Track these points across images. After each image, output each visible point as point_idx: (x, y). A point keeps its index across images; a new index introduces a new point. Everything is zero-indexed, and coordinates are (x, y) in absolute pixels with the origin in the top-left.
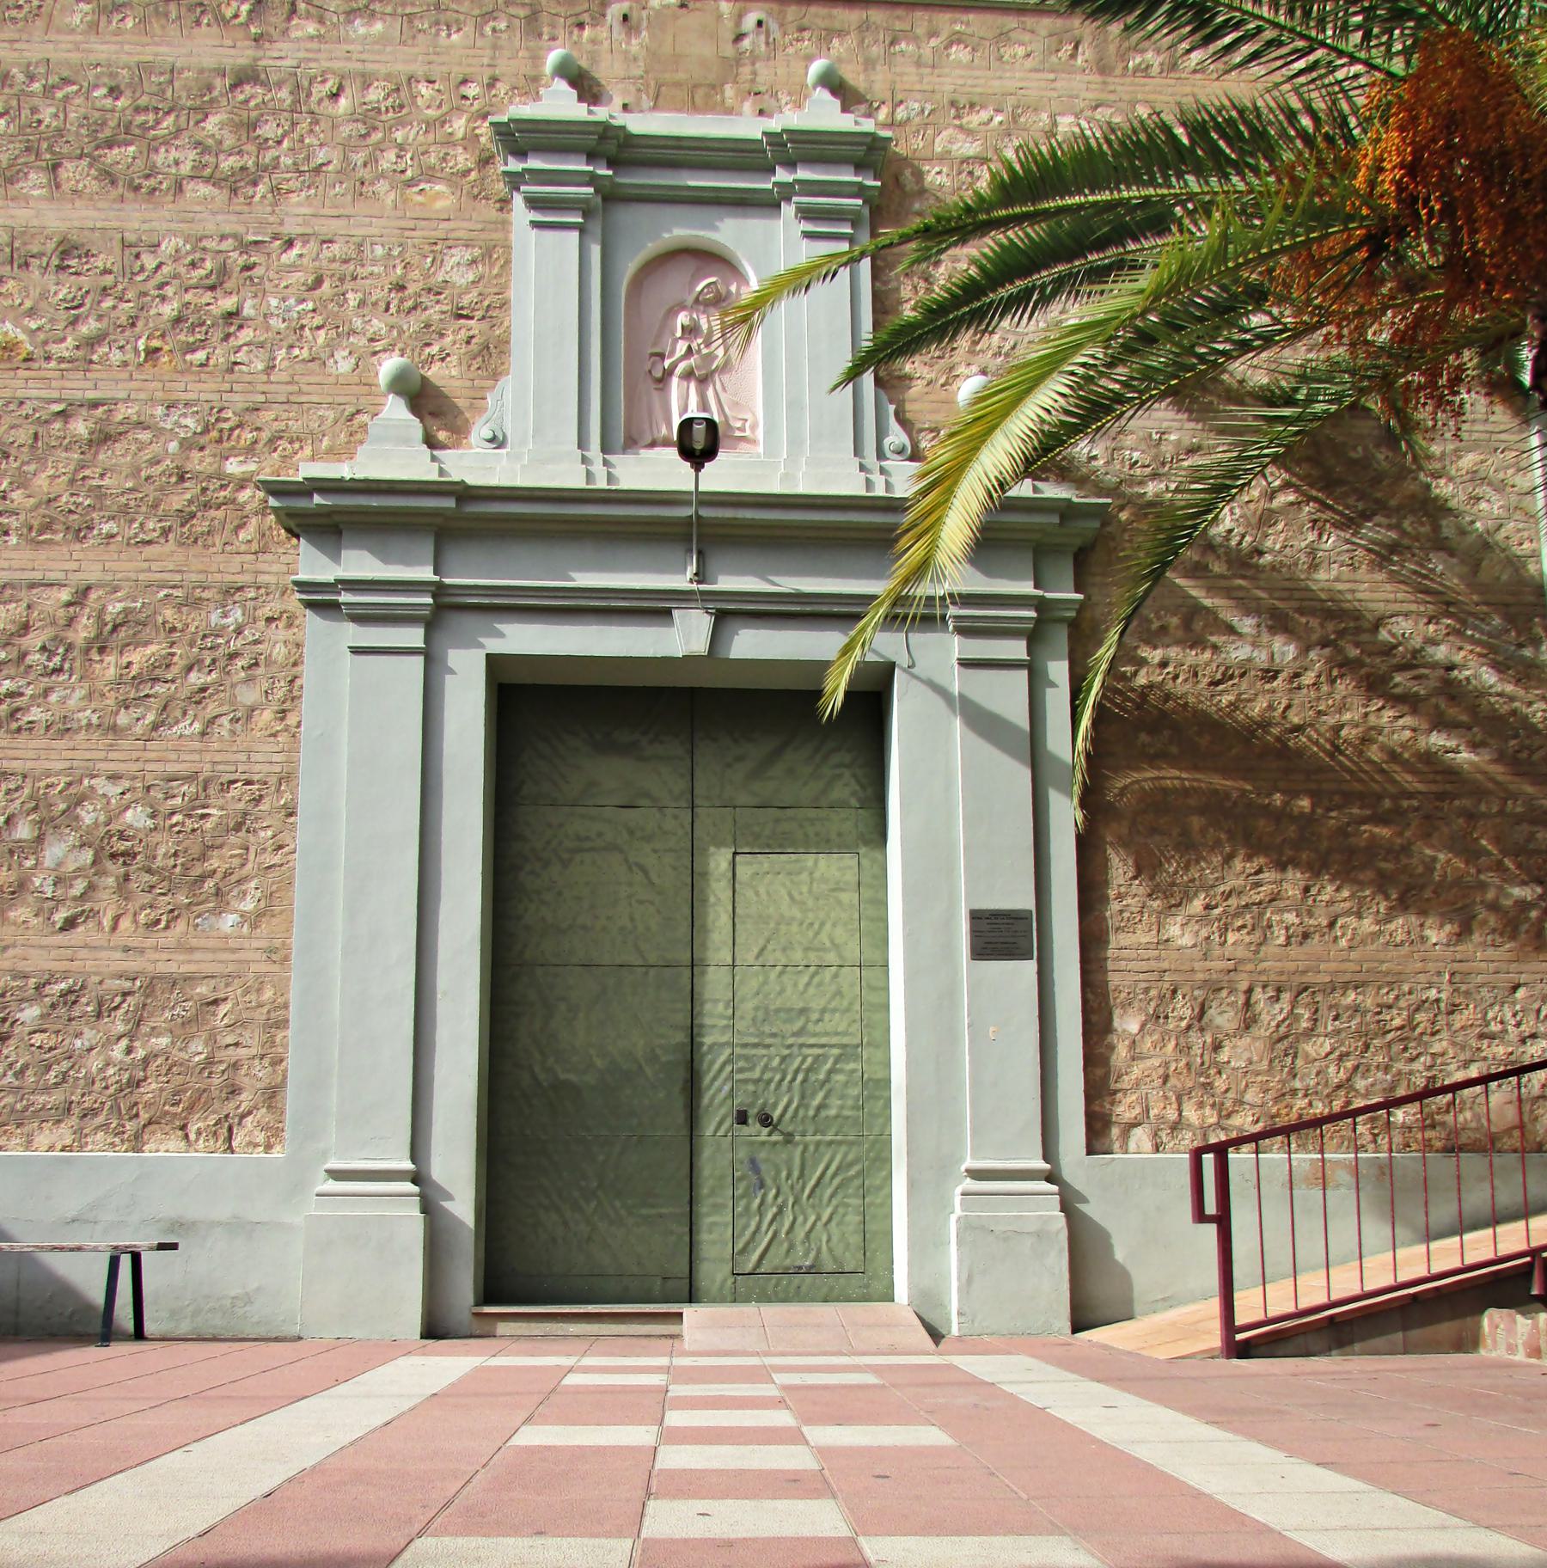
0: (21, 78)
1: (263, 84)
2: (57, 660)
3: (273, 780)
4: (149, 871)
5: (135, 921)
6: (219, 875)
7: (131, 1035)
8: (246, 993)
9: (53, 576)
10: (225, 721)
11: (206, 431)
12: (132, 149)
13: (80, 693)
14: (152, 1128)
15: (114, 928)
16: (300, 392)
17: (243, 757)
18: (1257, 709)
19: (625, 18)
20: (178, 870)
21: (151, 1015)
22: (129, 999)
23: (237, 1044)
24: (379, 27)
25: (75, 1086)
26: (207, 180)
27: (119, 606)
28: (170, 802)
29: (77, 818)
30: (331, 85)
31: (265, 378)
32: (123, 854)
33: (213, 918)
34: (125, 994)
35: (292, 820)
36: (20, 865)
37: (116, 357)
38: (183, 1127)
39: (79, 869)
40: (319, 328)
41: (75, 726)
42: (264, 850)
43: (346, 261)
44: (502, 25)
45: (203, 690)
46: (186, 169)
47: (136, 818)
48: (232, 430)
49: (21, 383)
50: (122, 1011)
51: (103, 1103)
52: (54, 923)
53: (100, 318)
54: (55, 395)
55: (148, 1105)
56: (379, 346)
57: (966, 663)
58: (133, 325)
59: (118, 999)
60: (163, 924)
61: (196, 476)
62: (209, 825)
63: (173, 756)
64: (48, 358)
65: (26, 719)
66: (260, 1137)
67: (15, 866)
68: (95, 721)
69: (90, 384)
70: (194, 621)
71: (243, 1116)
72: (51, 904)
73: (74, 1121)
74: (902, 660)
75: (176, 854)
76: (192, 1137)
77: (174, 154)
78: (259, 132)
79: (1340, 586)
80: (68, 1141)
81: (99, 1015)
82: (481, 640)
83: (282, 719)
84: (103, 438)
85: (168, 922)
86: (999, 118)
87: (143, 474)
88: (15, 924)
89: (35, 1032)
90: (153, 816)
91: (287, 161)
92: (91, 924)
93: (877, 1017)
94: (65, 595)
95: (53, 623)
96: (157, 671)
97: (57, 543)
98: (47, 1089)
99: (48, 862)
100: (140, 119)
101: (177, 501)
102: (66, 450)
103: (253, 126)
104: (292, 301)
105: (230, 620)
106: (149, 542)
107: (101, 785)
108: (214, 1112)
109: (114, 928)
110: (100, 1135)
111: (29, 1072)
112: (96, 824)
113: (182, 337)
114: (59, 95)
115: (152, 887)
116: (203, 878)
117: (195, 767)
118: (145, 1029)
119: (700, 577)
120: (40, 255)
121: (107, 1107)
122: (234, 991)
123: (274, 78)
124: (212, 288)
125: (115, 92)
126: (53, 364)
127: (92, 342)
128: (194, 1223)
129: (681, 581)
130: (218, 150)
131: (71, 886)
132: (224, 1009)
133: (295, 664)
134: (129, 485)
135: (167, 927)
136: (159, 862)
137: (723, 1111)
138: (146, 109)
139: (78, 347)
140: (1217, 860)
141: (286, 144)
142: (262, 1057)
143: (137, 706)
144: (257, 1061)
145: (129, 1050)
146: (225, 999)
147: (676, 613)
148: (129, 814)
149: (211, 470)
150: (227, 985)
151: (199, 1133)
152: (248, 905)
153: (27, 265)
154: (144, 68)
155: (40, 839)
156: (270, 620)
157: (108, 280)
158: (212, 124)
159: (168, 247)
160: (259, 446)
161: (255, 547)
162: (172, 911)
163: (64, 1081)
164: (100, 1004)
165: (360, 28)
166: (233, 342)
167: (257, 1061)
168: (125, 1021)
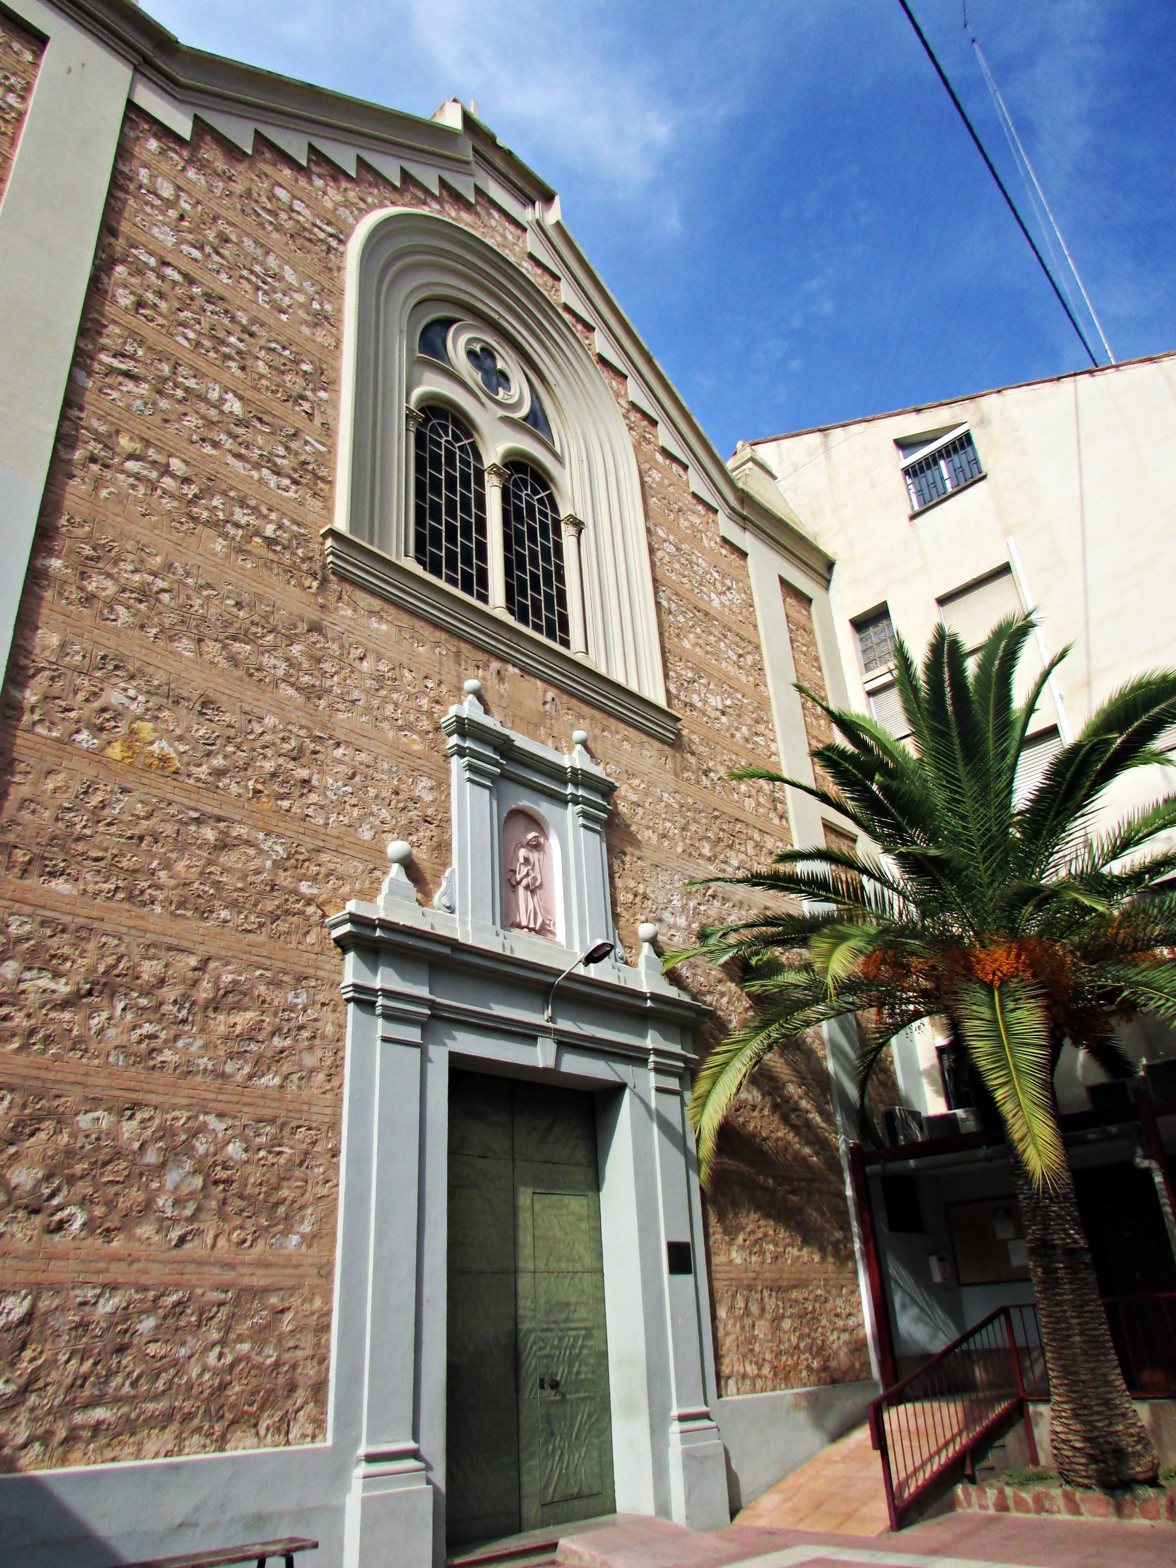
0: (181, 571)
1: (325, 636)
2: (185, 1012)
3: (324, 1128)
4: (241, 1196)
5: (229, 1240)
6: (287, 1203)
7: (222, 1342)
8: (304, 1301)
9: (185, 944)
10: (295, 1077)
11: (288, 858)
12: (248, 647)
13: (199, 1042)
14: (232, 1427)
15: (214, 1245)
16: (343, 846)
17: (305, 1107)
18: (751, 1126)
19: (499, 673)
20: (262, 1196)
21: (237, 1322)
22: (222, 1309)
23: (296, 1347)
24: (384, 627)
25: (177, 1393)
26: (292, 685)
27: (230, 977)
28: (258, 1140)
29: (193, 1147)
30: (359, 652)
31: (324, 830)
32: (224, 1182)
33: (283, 1239)
34: (221, 1304)
35: (334, 1160)
36: (147, 1186)
37: (235, 789)
38: (255, 1425)
39: (191, 1193)
40: (354, 806)
41: (195, 1069)
42: (317, 1183)
43: (368, 767)
44: (444, 652)
45: (282, 1052)
46: (280, 673)
47: (234, 1150)
48: (304, 861)
49: (170, 789)
50: (216, 1320)
51: (198, 1407)
52: (170, 1241)
53: (225, 757)
54: (192, 804)
55: (233, 1406)
56: (386, 827)
57: (659, 1090)
58: (246, 769)
59: (215, 1309)
60: (248, 1244)
61: (282, 888)
62: (282, 1160)
63: (261, 1102)
64: (189, 776)
65: (160, 1059)
66: (309, 1429)
67: (143, 1187)
68: (210, 1067)
69: (215, 803)
70: (278, 998)
71: (297, 1411)
72: (169, 1222)
73: (174, 1427)
74: (631, 1084)
75: (261, 1184)
76: (262, 1432)
77: (273, 661)
78: (322, 666)
79: (772, 1064)
80: (170, 1446)
81: (199, 1326)
82: (447, 1041)
83: (329, 1081)
84: (223, 845)
85: (253, 1241)
86: (643, 785)
87: (249, 879)
88: (139, 1239)
89: (149, 1342)
90: (246, 1150)
91: (337, 690)
92: (196, 1242)
93: (600, 1307)
94: (193, 961)
95: (183, 981)
96: (253, 1033)
97: (188, 918)
98: (156, 1398)
99: (169, 1185)
100: (254, 629)
101: (270, 905)
102: (199, 848)
103: (319, 661)
104: (340, 784)
105: (299, 1001)
106: (250, 931)
107: (212, 1121)
108: (279, 1409)
109: (214, 1245)
110: (196, 1437)
111: (142, 1381)
112: (207, 1154)
113: (276, 787)
114: (205, 593)
115: (242, 1210)
116: (277, 1204)
117: (276, 1112)
118: (232, 1336)
119: (551, 1019)
120: (189, 700)
121: (201, 1412)
122: (295, 1301)
123: (330, 635)
124: (294, 759)
125: (239, 605)
126: (192, 781)
127: (219, 773)
128: (270, 1515)
129: (540, 1019)
130: (297, 666)
131: (184, 1208)
132: (288, 1316)
133: (338, 1040)
134: (240, 885)
135: (251, 1246)
136: (249, 1190)
137: (532, 1380)
138: (257, 624)
139: (210, 774)
140: (745, 1212)
141: (336, 678)
142: (312, 1358)
143: (239, 1059)
144: (309, 1362)
145: (221, 1356)
146: (289, 1308)
147: (540, 1039)
148: (230, 1147)
149: (291, 886)
150: (291, 1296)
151: (268, 1429)
152: (306, 1228)
153: (178, 703)
154: (260, 598)
155: (163, 1165)
156: (323, 1004)
157: (232, 732)
158: (296, 649)
159: (270, 721)
160: (320, 877)
161: (317, 949)
162: (255, 1232)
163: (170, 1388)
164: (201, 1315)
165: (374, 623)
166: (304, 800)
167: (309, 1362)
168: (219, 1329)
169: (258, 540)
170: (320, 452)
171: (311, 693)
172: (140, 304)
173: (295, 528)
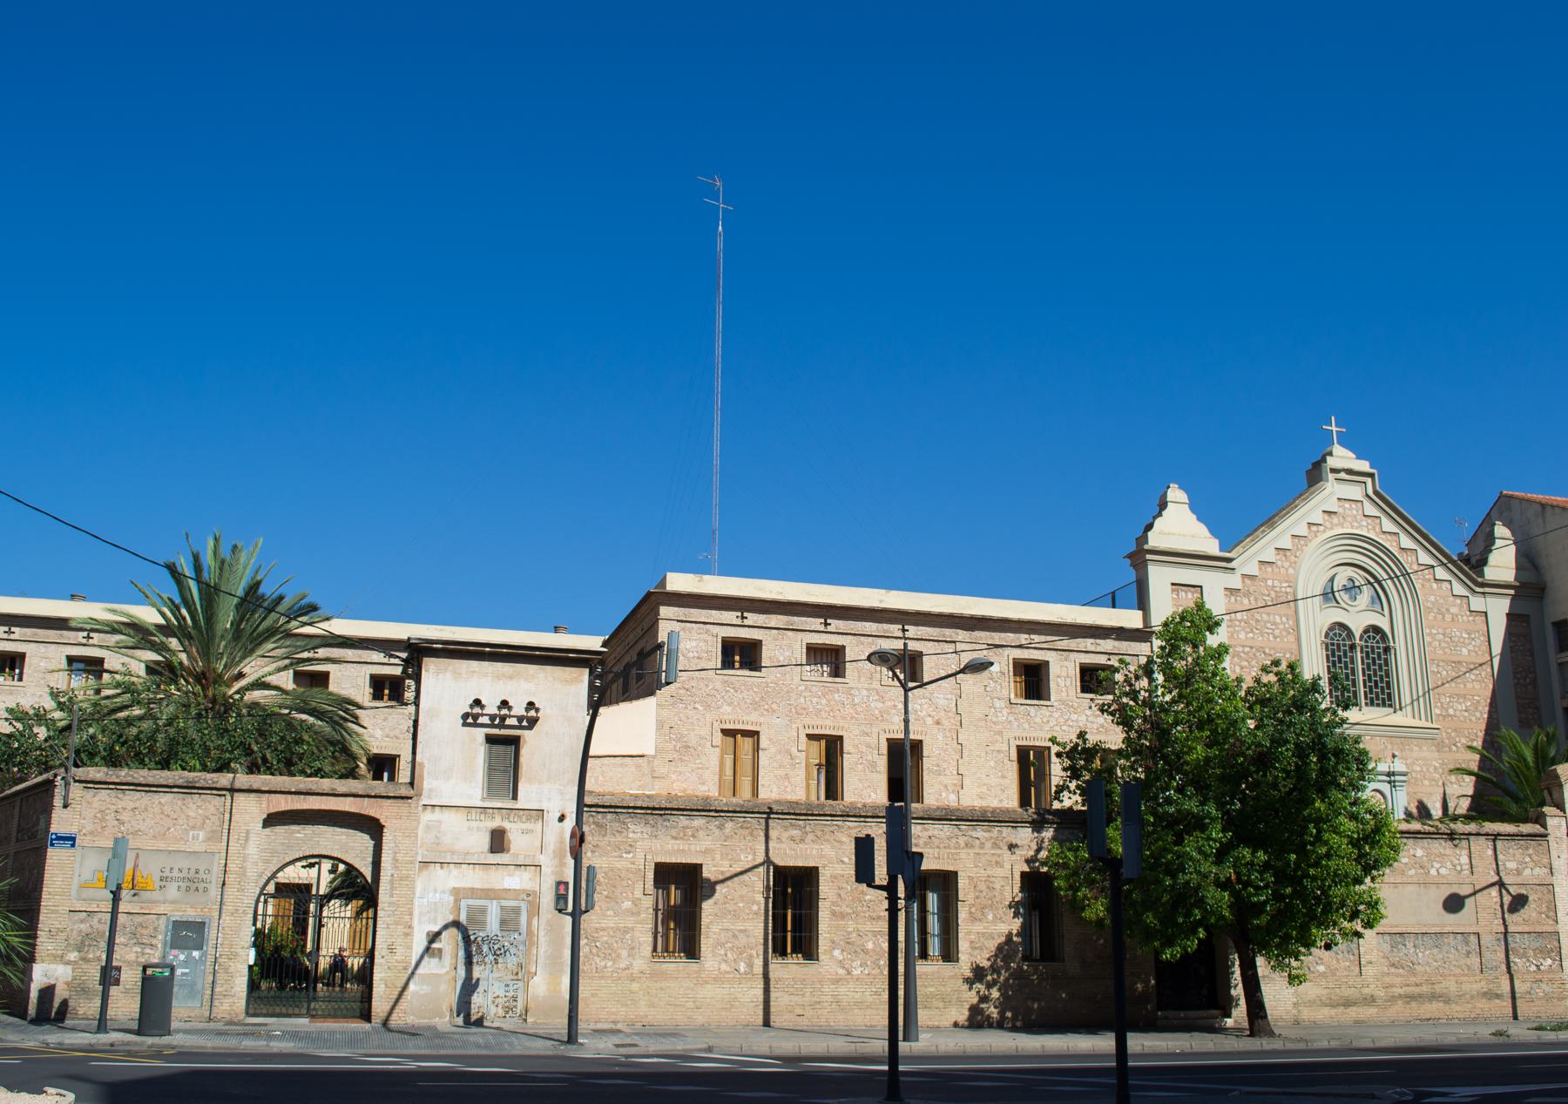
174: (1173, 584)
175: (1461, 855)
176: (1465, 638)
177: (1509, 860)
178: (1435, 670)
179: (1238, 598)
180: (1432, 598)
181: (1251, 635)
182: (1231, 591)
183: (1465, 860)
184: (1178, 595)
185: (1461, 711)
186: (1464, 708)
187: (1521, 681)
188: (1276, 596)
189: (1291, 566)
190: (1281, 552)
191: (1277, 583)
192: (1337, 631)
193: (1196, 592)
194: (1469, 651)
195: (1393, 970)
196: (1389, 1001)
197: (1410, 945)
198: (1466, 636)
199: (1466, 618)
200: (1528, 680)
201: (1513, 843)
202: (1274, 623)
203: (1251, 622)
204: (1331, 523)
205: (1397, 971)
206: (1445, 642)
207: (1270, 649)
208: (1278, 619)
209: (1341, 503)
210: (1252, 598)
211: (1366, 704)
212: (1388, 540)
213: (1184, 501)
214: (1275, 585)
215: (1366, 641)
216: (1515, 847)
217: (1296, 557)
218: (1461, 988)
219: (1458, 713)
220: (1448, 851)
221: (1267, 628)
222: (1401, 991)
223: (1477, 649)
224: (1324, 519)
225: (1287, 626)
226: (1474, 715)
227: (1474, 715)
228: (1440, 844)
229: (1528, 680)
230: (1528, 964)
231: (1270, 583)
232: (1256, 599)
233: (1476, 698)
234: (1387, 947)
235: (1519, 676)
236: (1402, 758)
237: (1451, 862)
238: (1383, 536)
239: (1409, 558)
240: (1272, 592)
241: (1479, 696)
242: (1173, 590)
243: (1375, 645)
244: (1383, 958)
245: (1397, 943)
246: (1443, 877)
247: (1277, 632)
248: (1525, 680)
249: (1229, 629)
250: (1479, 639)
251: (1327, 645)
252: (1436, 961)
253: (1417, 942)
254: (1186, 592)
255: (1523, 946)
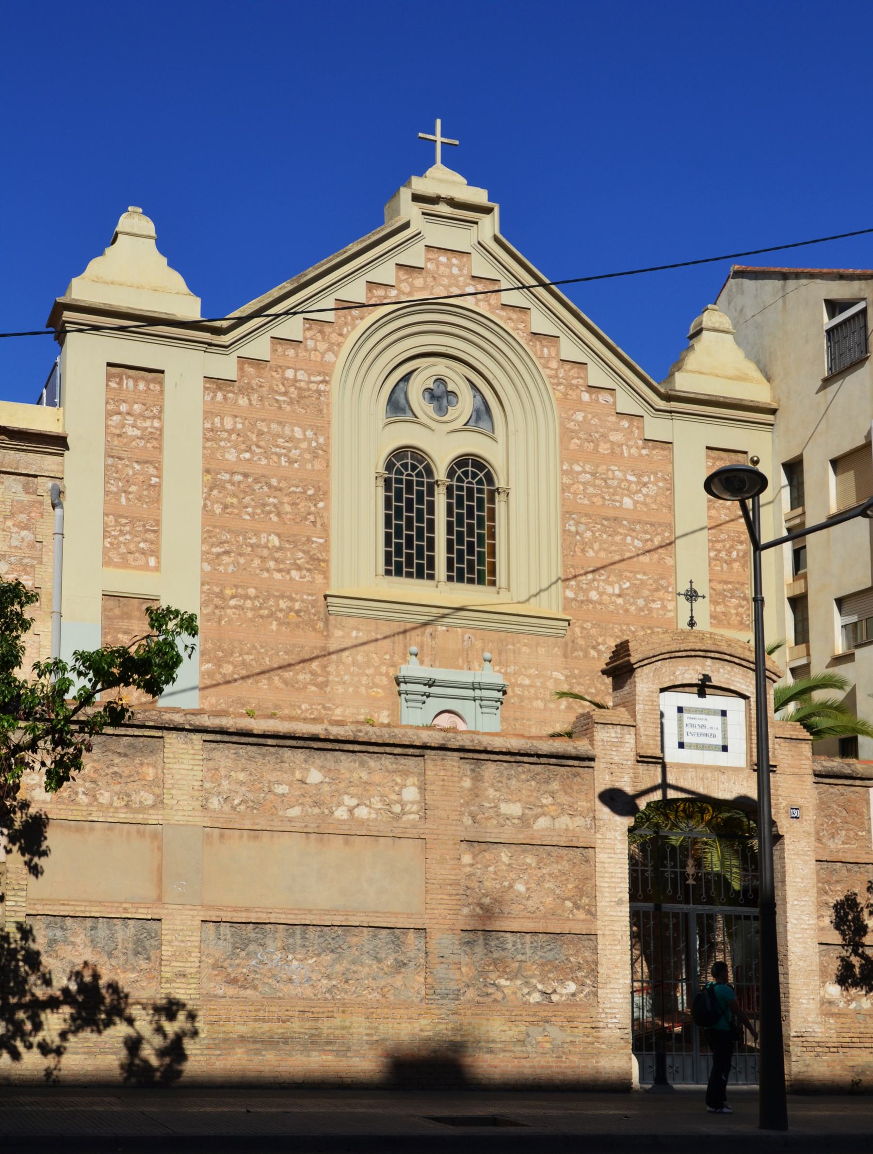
169: (292, 614)
170: (321, 544)
171: (322, 686)
172: (226, 507)
173: (310, 598)
174: (109, 365)
175: (405, 786)
176: (630, 482)
177: (507, 801)
178: (573, 529)
179: (230, 395)
180: (580, 416)
181: (247, 455)
182: (215, 383)
183: (411, 793)
184: (120, 383)
185: (610, 595)
186: (617, 591)
187: (723, 554)
188: (300, 397)
189: (330, 349)
190: (316, 327)
191: (301, 375)
192: (409, 461)
193: (153, 381)
194: (636, 503)
195: (231, 991)
196: (217, 1047)
197: (271, 945)
198: (633, 479)
199: (632, 450)
200: (734, 554)
201: (520, 769)
202: (291, 439)
203: (249, 434)
204: (412, 286)
205: (242, 993)
206: (594, 486)
207: (279, 482)
208: (298, 433)
209: (431, 255)
210: (255, 397)
211: (450, 579)
212: (510, 319)
213: (146, 233)
214: (299, 378)
215: (459, 480)
216: (523, 777)
217: (341, 335)
218: (376, 1028)
219: (605, 598)
220: (377, 778)
221: (277, 446)
222: (242, 1029)
223: (648, 500)
224: (397, 277)
225: (314, 444)
226: (634, 603)
227: (634, 603)
228: (362, 764)
229: (734, 554)
230: (526, 990)
231: (290, 374)
232: (261, 399)
233: (639, 576)
234: (220, 949)
235: (718, 546)
236: (500, 663)
237: (383, 796)
238: (503, 313)
239: (546, 350)
240: (292, 389)
241: (644, 574)
242: (109, 377)
243: (475, 486)
244: (215, 966)
245: (248, 941)
246: (362, 822)
247: (295, 453)
248: (729, 553)
249: (209, 444)
250: (655, 483)
251: (388, 482)
252: (328, 977)
253: (291, 941)
254: (136, 381)
255: (520, 957)
